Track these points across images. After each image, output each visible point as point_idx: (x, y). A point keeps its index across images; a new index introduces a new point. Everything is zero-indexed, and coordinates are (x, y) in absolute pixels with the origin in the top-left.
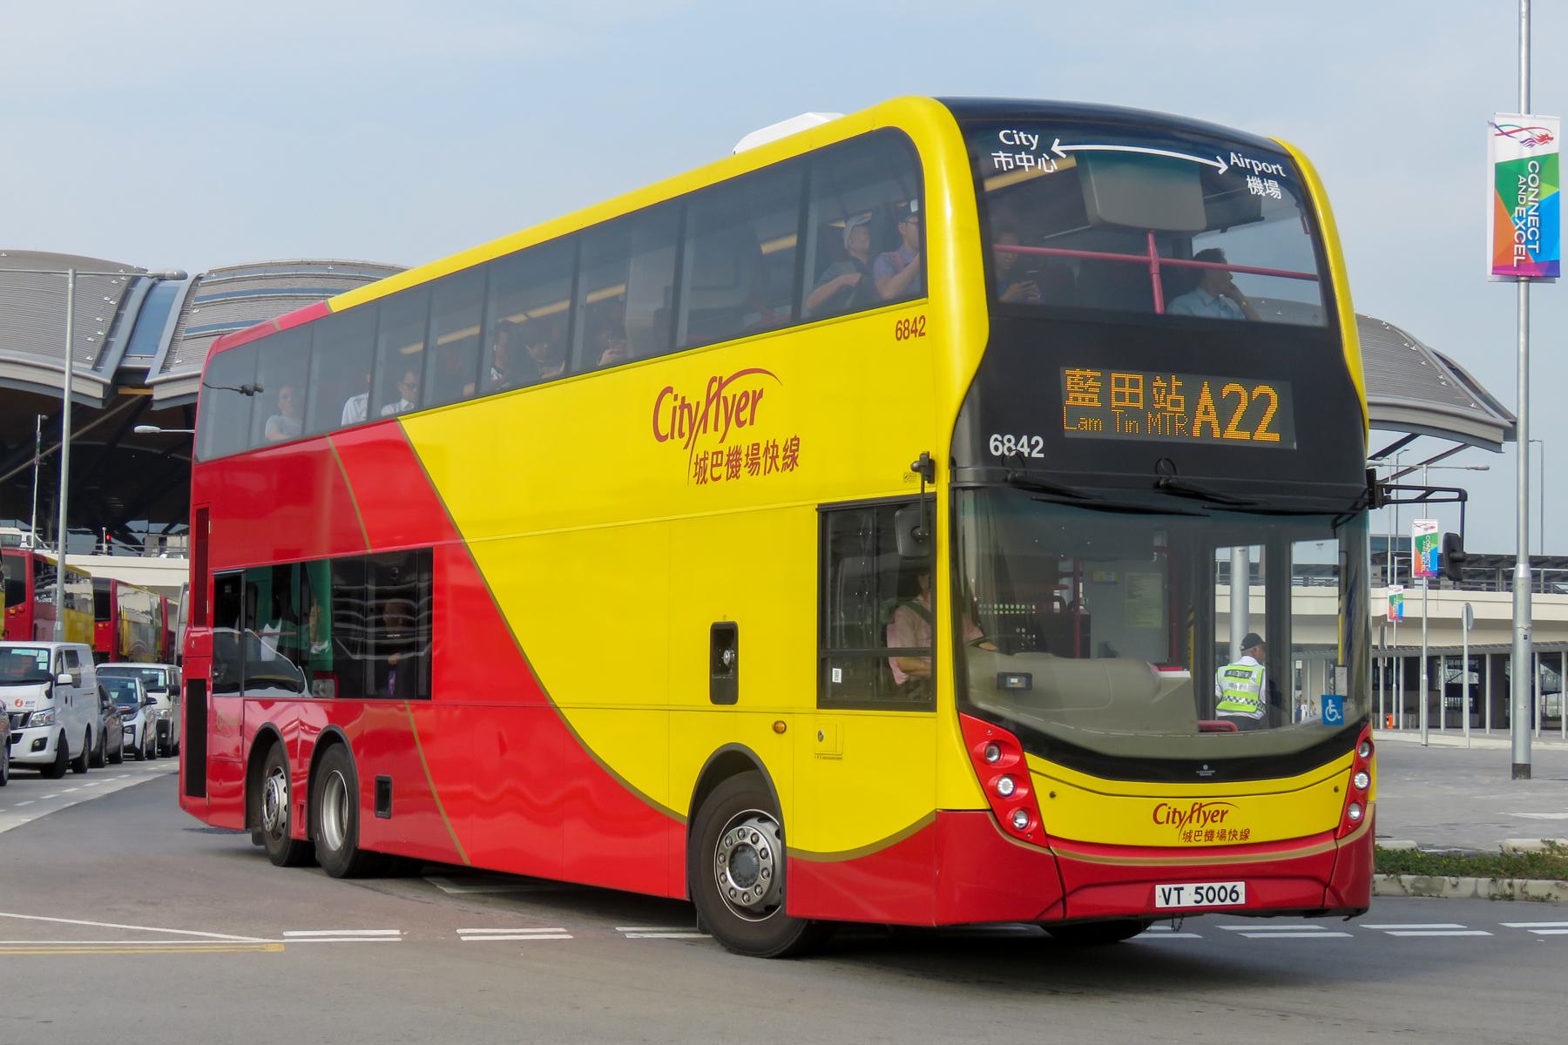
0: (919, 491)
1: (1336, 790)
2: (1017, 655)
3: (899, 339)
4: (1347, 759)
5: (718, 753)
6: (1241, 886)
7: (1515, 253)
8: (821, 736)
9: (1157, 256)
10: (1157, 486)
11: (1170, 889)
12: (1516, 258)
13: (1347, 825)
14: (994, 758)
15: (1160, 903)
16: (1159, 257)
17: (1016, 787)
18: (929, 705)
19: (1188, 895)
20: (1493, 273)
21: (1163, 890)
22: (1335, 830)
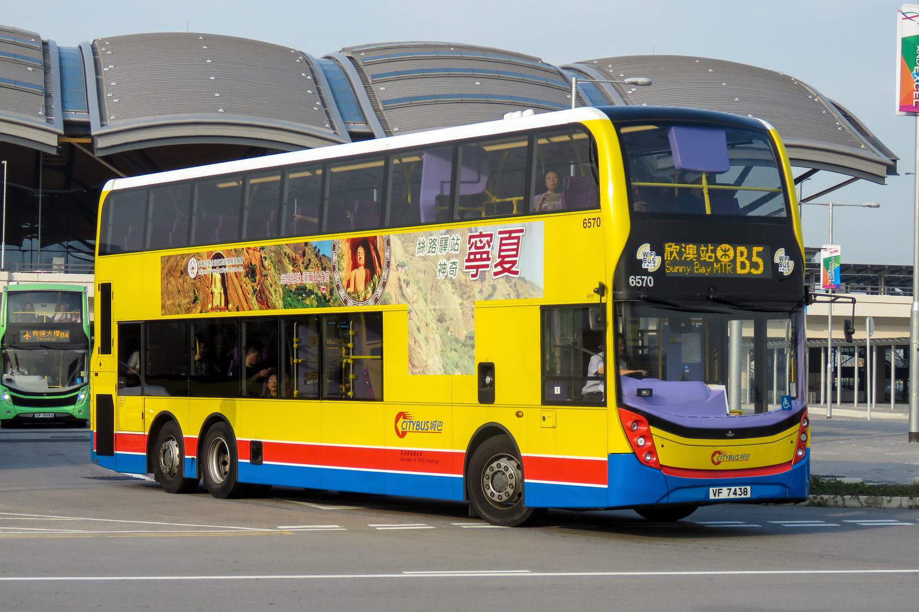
0: (599, 302)
1: (792, 442)
2: (643, 380)
3: (585, 228)
4: (797, 427)
5: (485, 426)
6: (749, 488)
7: (914, 97)
8: (544, 419)
9: (707, 185)
10: (708, 298)
11: (716, 490)
12: (915, 100)
13: (797, 459)
14: (636, 428)
15: (712, 497)
16: (708, 184)
17: (645, 442)
18: (604, 404)
19: (725, 493)
20: (900, 111)
21: (713, 490)
22: (791, 461)
